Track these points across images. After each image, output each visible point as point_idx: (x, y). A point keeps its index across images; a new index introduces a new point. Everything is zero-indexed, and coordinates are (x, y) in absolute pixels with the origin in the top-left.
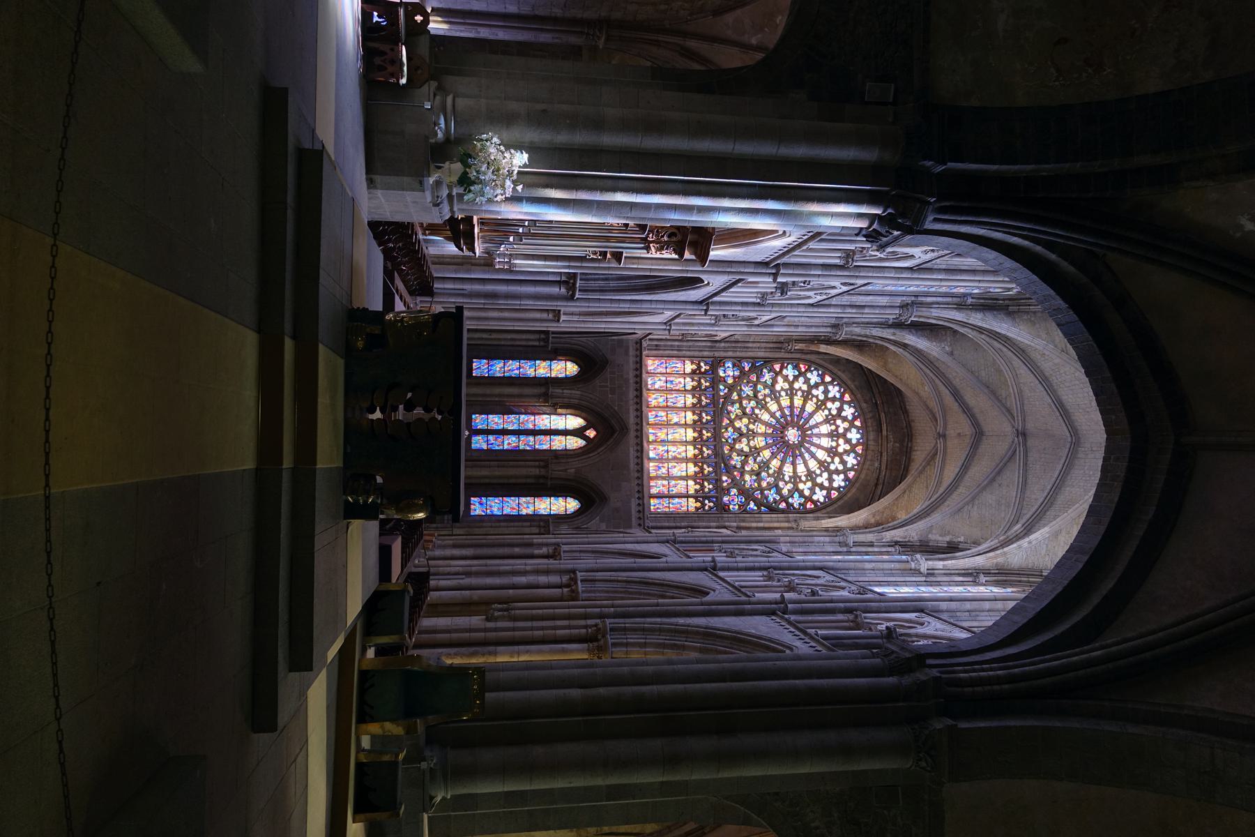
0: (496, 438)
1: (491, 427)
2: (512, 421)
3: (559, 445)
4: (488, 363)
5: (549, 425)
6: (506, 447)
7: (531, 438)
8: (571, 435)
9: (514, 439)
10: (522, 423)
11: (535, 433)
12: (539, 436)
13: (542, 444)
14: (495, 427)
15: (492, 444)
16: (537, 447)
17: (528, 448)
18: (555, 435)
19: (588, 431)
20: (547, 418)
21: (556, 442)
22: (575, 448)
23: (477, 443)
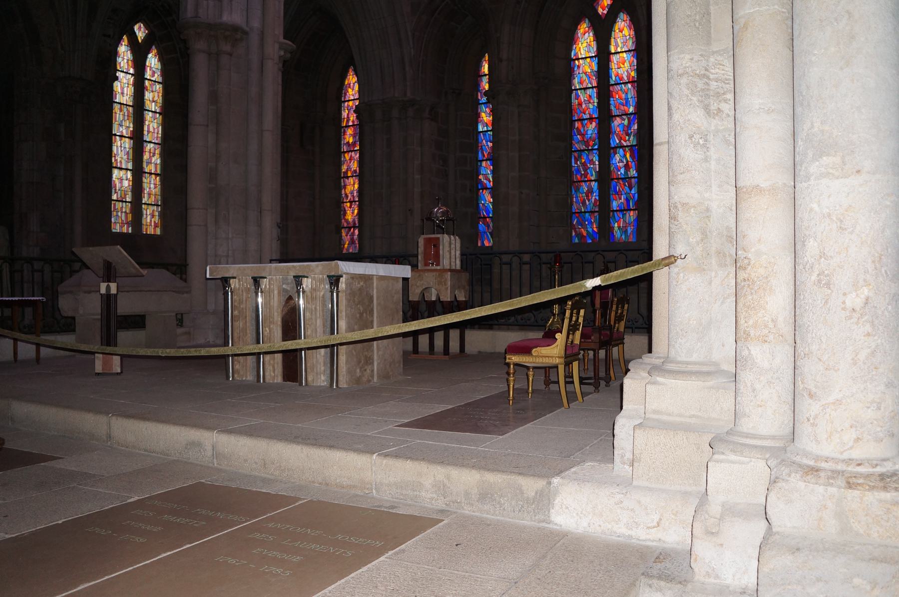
0: (617, 193)
1: (595, 204)
2: (584, 164)
3: (627, 64)
4: (485, 218)
5: (589, 92)
6: (633, 172)
7: (617, 124)
8: (608, 43)
9: (618, 157)
10: (587, 143)
11: (605, 116)
12: (612, 108)
13: (627, 99)
14: (595, 196)
15: (627, 200)
16: (631, 110)
17: (636, 127)
18: (608, 76)
19: (600, 11)
20: (577, 97)
21: (620, 71)
22: (632, 33)
23: (626, 232)
